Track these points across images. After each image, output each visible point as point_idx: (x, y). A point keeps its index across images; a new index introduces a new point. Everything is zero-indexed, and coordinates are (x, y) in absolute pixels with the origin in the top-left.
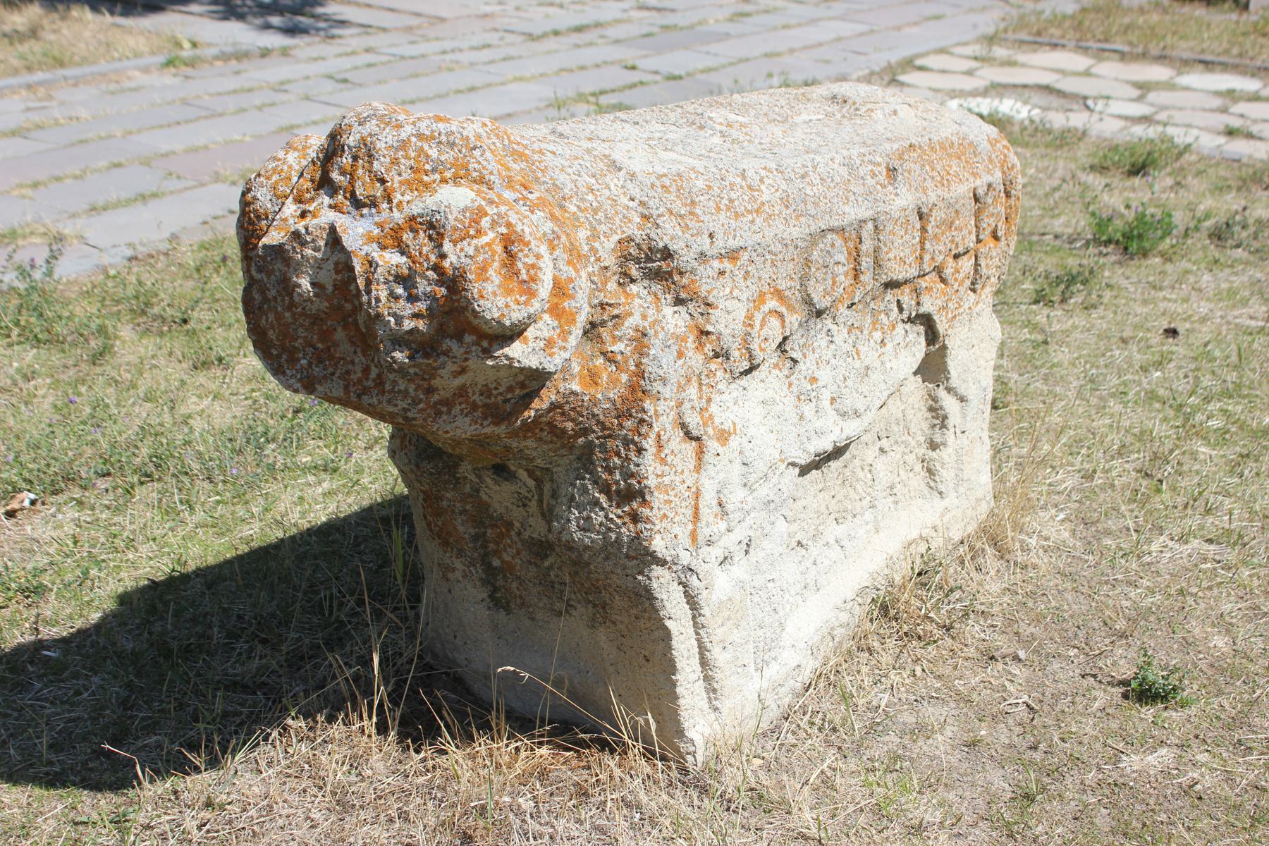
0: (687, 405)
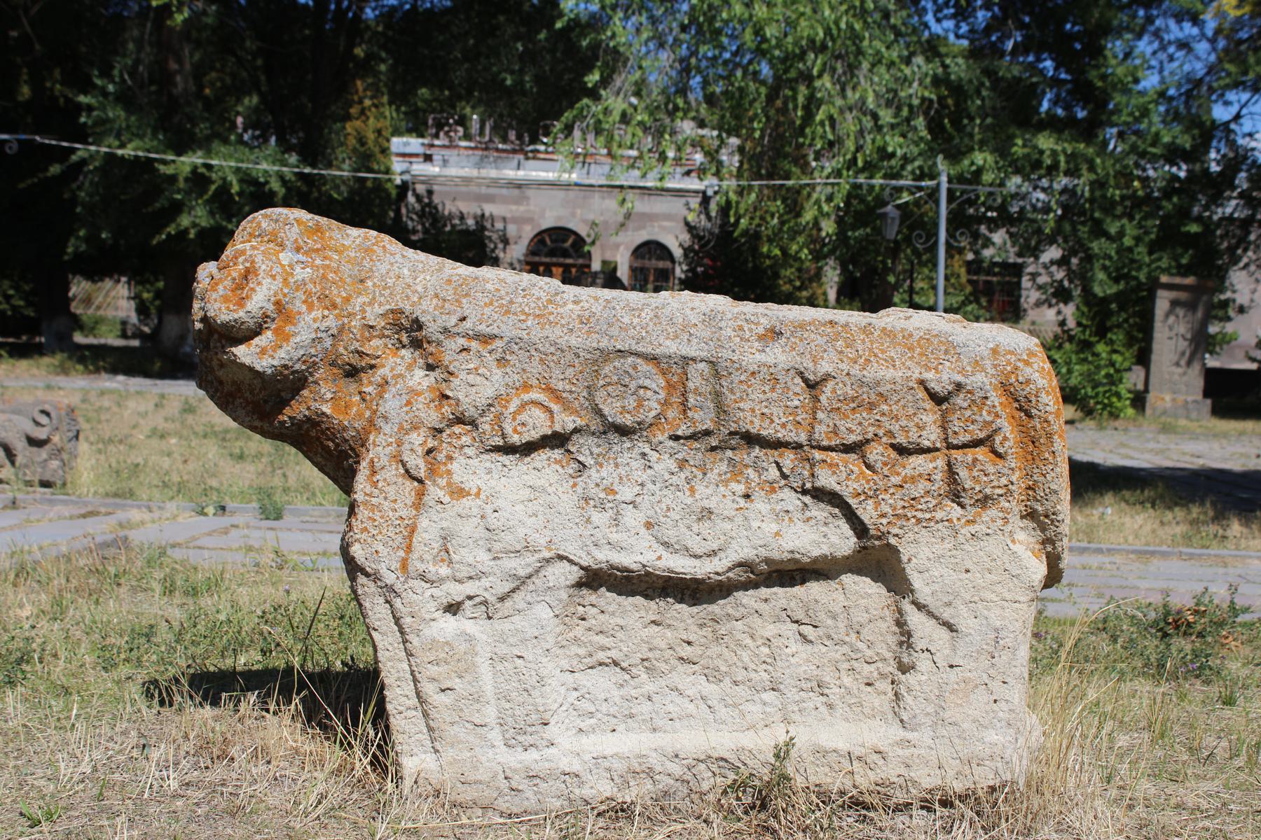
0: (406, 446)
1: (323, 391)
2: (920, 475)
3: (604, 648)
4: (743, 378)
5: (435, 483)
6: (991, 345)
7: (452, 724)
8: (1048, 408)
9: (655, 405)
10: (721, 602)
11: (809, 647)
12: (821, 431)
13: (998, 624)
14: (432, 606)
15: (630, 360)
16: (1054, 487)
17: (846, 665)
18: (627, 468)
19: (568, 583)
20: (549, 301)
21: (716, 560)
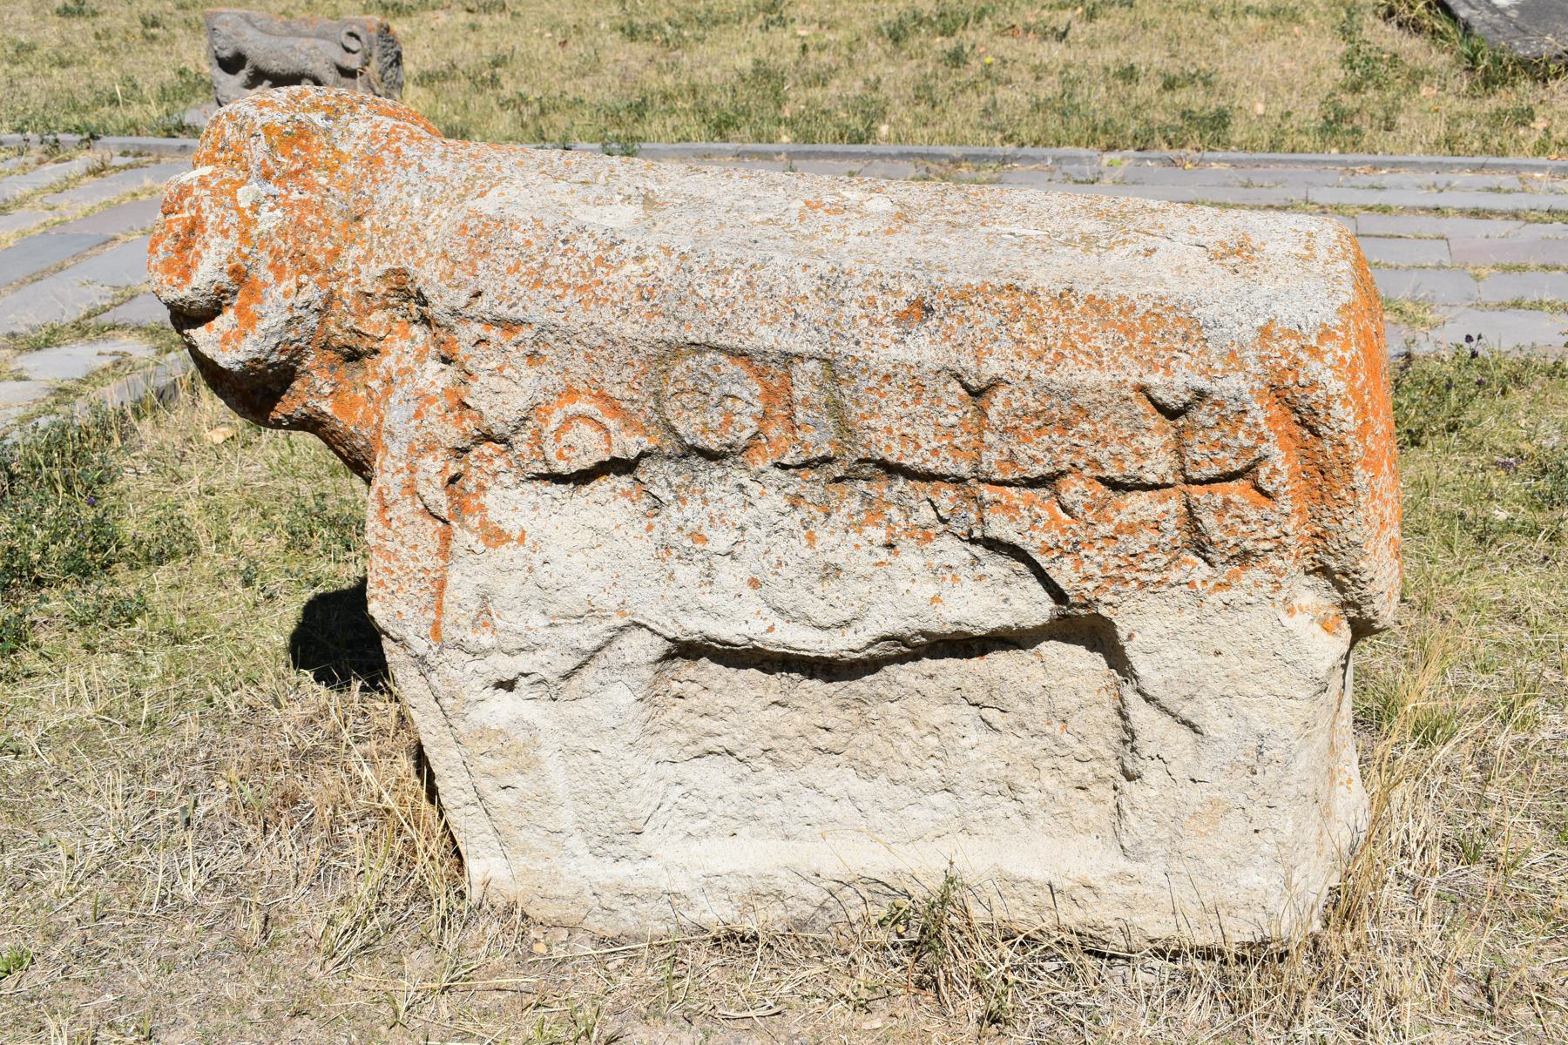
0: (420, 475)
1: (318, 384)
2: (1142, 522)
3: (710, 734)
4: (872, 383)
5: (463, 524)
6: (1261, 322)
7: (521, 828)
8: (1344, 426)
9: (749, 421)
10: (868, 678)
11: (995, 737)
12: (991, 461)
13: (1263, 728)
14: (476, 685)
15: (710, 356)
16: (1354, 538)
17: (1048, 763)
18: (719, 505)
19: (650, 659)
20: (600, 261)
21: (849, 632)
